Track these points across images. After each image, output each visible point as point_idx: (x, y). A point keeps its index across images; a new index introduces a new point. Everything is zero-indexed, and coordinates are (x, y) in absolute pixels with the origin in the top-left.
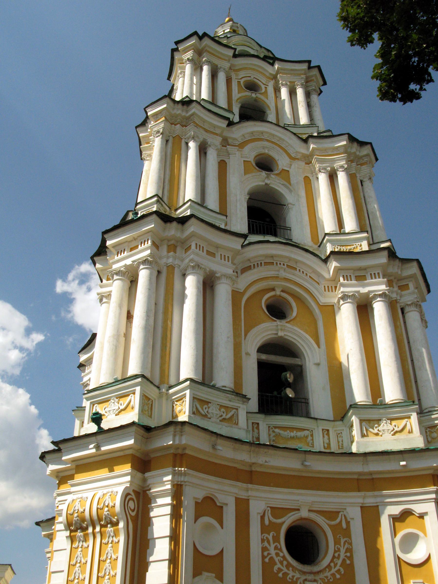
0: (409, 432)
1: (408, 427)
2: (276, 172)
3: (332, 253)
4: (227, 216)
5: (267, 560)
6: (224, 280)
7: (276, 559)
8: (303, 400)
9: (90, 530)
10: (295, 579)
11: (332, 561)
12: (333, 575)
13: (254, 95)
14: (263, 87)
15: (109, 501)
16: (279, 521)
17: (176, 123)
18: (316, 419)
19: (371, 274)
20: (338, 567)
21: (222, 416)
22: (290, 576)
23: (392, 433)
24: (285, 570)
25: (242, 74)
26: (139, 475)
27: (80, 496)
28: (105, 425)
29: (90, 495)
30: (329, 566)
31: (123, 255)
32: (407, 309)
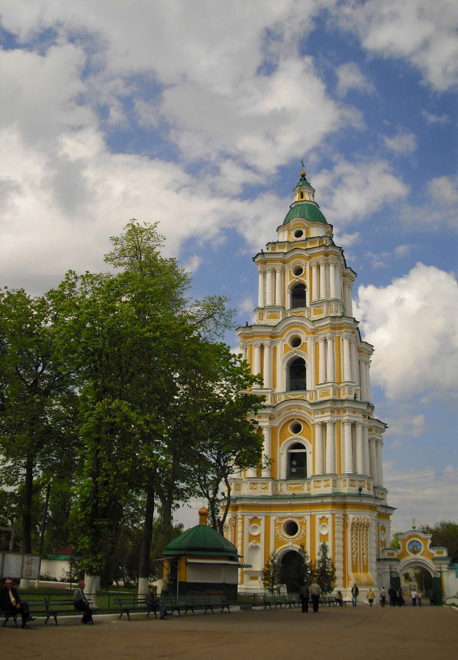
6: (265, 429)
7: (280, 535)
11: (299, 534)
25: (291, 263)
26: (234, 512)
30: (297, 536)
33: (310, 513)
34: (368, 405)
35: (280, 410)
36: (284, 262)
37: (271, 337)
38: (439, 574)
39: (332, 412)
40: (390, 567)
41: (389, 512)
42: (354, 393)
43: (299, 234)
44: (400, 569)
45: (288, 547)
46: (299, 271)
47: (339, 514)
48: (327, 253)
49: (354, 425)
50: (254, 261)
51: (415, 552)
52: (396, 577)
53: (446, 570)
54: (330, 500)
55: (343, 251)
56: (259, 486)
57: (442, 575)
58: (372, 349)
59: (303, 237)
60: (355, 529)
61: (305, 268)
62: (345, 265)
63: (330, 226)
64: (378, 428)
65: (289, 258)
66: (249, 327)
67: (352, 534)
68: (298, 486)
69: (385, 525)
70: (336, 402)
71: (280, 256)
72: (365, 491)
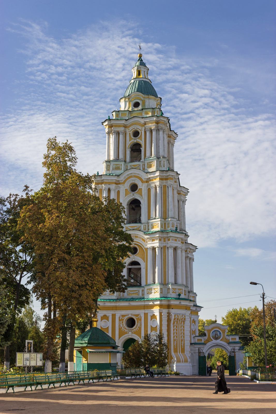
1: (158, 291)
5: (120, 328)
7: (122, 327)
11: (136, 327)
12: (136, 330)
16: (123, 318)
24: (124, 329)
25: (131, 128)
34: (185, 235)
36: (125, 126)
37: (116, 184)
38: (233, 353)
39: (160, 240)
40: (199, 349)
41: (198, 309)
42: (175, 226)
43: (136, 105)
44: (206, 350)
46: (136, 134)
47: (165, 311)
48: (158, 121)
49: (175, 249)
50: (103, 124)
51: (216, 338)
52: (203, 356)
53: (237, 350)
54: (158, 303)
55: (169, 120)
57: (235, 354)
58: (188, 191)
59: (140, 107)
60: (176, 323)
61: (141, 132)
62: (170, 128)
63: (159, 99)
64: (191, 249)
66: (100, 176)
67: (174, 326)
68: (136, 292)
69: (195, 319)
70: (163, 233)
71: (123, 122)
72: (182, 296)
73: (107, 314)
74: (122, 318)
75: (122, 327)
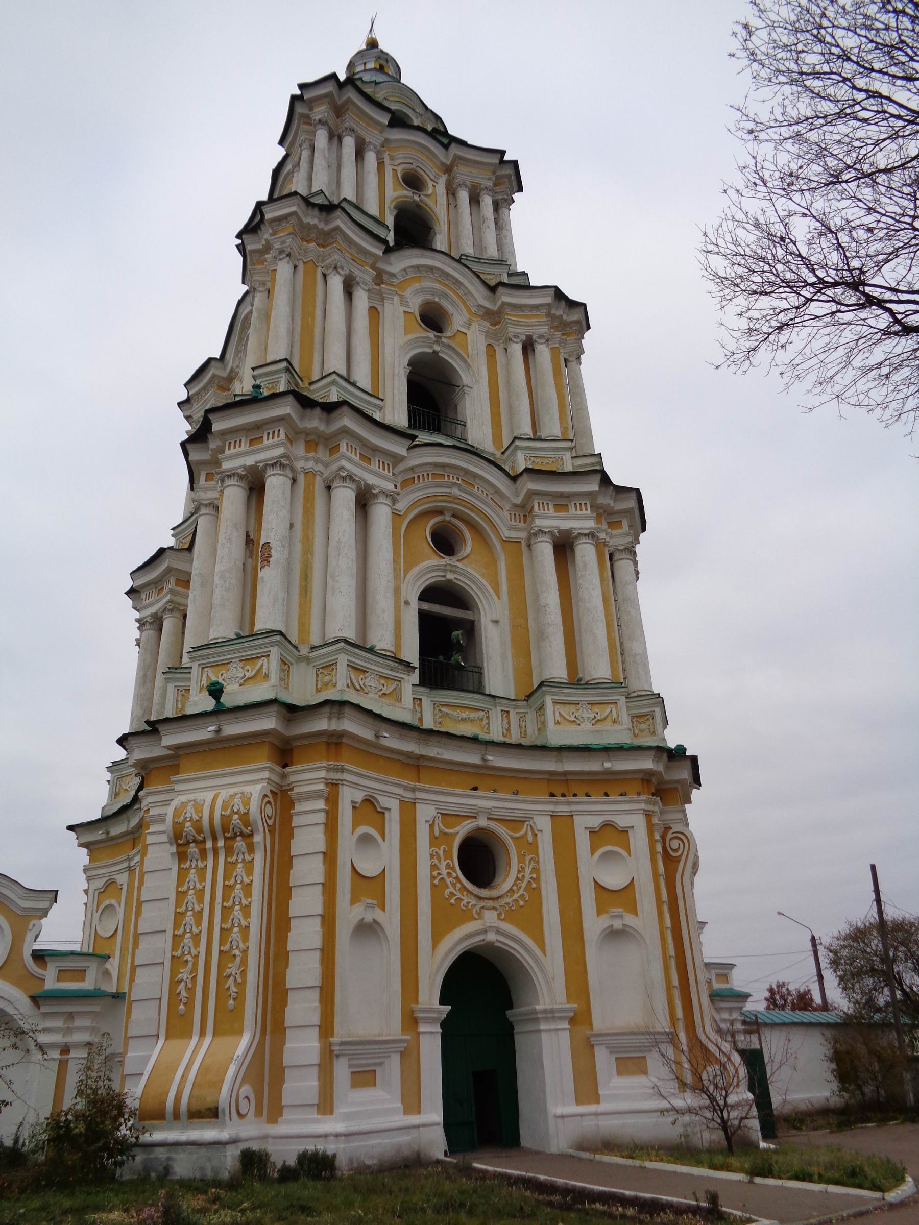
0: (614, 722)
2: (449, 334)
3: (527, 470)
4: (382, 400)
5: (436, 882)
6: (382, 499)
7: (449, 880)
8: (477, 670)
9: (209, 845)
10: (470, 907)
11: (515, 884)
13: (416, 198)
14: (430, 184)
15: (239, 805)
17: (309, 238)
18: (494, 697)
19: (575, 504)
20: (521, 892)
21: (381, 690)
22: (464, 902)
23: (594, 721)
24: (459, 895)
26: (278, 769)
27: (191, 797)
28: (227, 700)
29: (208, 796)
30: (511, 891)
31: (238, 449)
32: (617, 556)
33: (551, 808)
35: (412, 469)
45: (485, 932)
56: (371, 682)
65: (396, 140)
73: (379, 798)
74: (447, 831)
75: (444, 875)
